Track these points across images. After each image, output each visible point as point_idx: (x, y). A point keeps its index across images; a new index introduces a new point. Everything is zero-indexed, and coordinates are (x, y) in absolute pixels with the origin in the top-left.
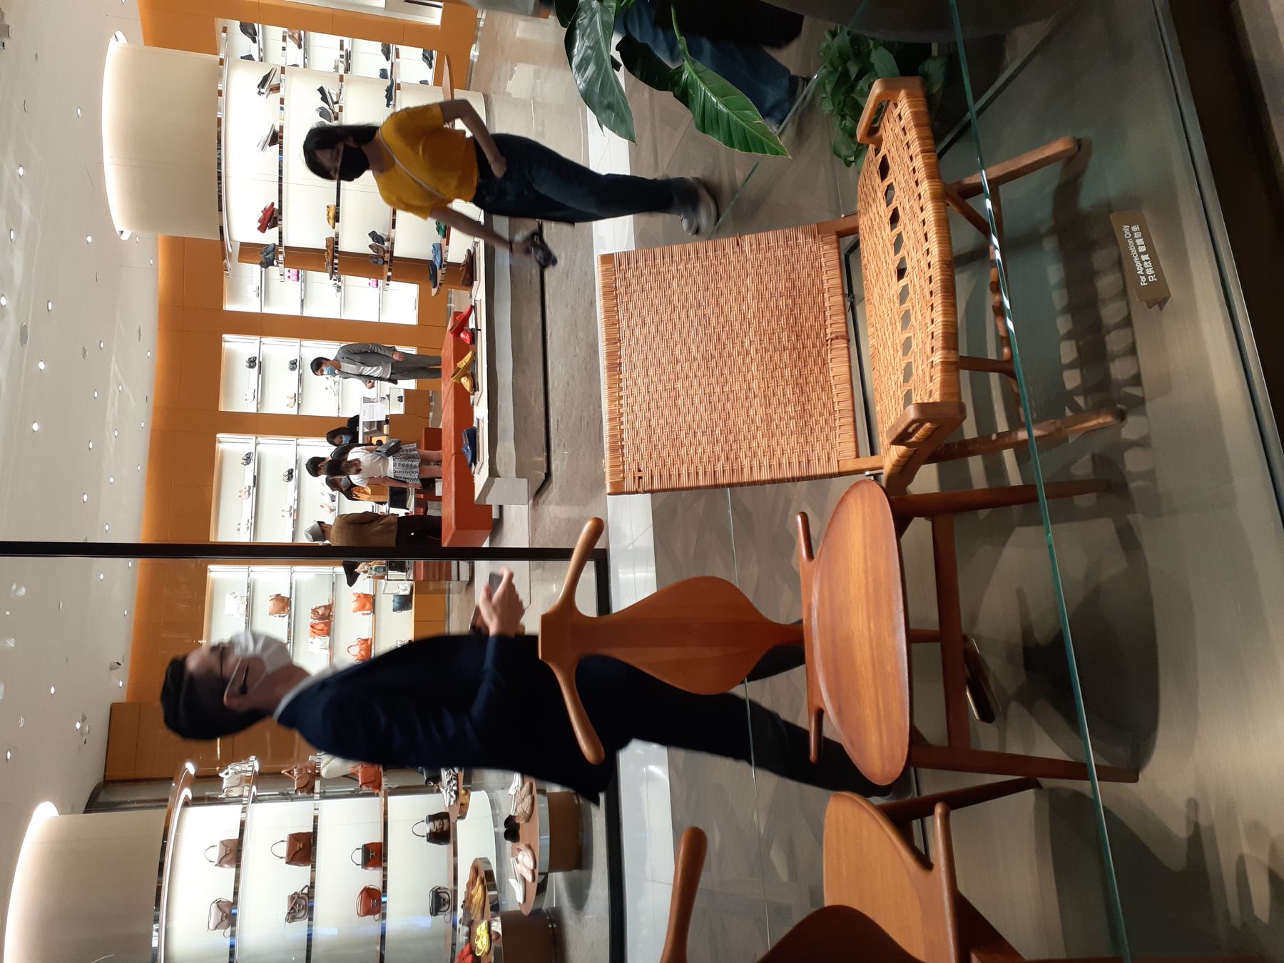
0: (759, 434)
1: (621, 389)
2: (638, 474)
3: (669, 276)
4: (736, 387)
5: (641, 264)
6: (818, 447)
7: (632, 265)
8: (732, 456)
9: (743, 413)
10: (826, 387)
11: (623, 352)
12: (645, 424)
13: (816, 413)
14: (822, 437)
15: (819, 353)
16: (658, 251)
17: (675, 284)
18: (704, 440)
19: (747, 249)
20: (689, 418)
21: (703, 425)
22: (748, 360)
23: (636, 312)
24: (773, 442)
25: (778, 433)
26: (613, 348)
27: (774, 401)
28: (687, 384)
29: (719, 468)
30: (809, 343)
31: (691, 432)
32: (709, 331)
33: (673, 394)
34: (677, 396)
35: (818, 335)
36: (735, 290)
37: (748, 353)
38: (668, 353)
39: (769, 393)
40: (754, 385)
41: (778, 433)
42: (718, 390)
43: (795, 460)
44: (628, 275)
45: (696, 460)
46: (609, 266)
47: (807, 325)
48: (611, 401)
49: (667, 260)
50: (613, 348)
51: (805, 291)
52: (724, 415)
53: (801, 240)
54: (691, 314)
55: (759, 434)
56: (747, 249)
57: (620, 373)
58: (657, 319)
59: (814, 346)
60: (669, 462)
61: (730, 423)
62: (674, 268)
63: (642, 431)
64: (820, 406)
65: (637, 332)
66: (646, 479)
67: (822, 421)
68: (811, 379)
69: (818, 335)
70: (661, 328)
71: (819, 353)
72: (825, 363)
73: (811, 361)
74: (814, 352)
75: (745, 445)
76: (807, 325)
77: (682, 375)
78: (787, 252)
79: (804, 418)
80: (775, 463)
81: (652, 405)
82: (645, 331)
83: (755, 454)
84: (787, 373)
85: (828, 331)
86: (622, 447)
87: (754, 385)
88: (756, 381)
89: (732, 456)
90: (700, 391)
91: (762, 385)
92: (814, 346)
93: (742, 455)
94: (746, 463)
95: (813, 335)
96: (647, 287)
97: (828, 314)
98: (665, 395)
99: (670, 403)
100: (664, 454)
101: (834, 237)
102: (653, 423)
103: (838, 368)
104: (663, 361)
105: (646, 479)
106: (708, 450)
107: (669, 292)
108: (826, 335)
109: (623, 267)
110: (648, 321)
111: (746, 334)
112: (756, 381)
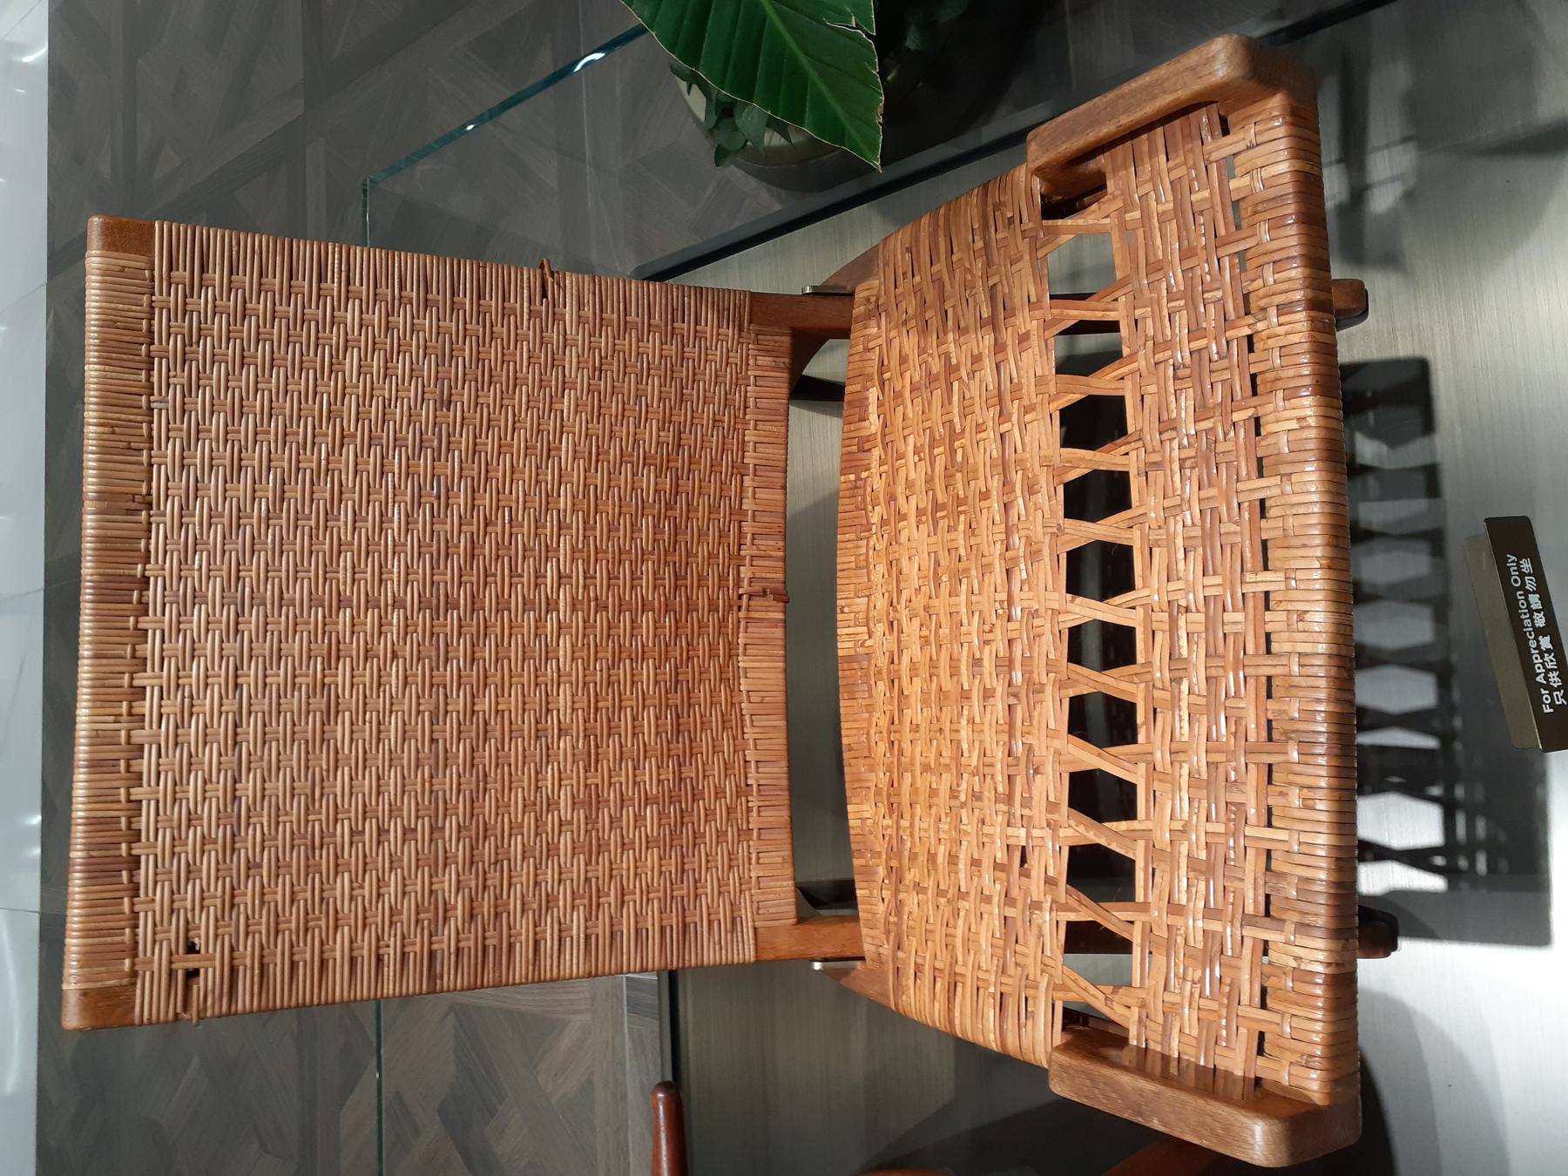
0: (565, 842)
1: (140, 663)
2: (186, 963)
3: (335, 336)
4: (513, 701)
5: (246, 279)
6: (710, 886)
7: (216, 275)
8: (486, 908)
9: (526, 777)
10: (732, 722)
11: (157, 540)
12: (219, 788)
13: (709, 793)
14: (721, 859)
15: (722, 623)
16: (307, 251)
17: (352, 361)
18: (408, 854)
19: (569, 313)
20: (367, 783)
21: (409, 807)
22: (550, 623)
23: (217, 423)
24: (601, 869)
25: (613, 840)
26: (123, 526)
27: (611, 748)
28: (367, 675)
29: (446, 940)
30: (703, 602)
31: (370, 828)
32: (448, 526)
33: (319, 702)
34: (331, 713)
35: (722, 579)
36: (528, 419)
37: (552, 606)
38: (313, 566)
39: (601, 725)
40: (563, 698)
41: (613, 840)
42: (459, 703)
43: (652, 924)
44: (200, 302)
45: (380, 914)
46: (134, 261)
47: (702, 552)
48: (101, 700)
49: (333, 286)
50: (123, 526)
51: (705, 462)
52: (469, 785)
53: (708, 329)
54: (396, 461)
55: (565, 842)
56: (569, 313)
57: (143, 609)
58: (283, 461)
59: (713, 608)
60: (293, 918)
61: (488, 805)
62: (351, 315)
63: (207, 811)
64: (716, 770)
65: (214, 484)
66: (211, 977)
67: (720, 810)
68: (702, 695)
69: (722, 579)
70: (295, 491)
71: (722, 623)
72: (731, 655)
73: (702, 646)
74: (712, 622)
75: (524, 872)
76: (702, 552)
77: (354, 646)
78: (672, 350)
79: (680, 798)
80: (601, 928)
81: (250, 729)
82: (243, 488)
83: (551, 900)
84: (647, 669)
85: (745, 572)
86: (134, 862)
87: (563, 698)
88: (565, 690)
89: (486, 908)
90: (407, 703)
91: (582, 702)
92: (713, 608)
93: (515, 905)
94: (524, 927)
95: (712, 580)
96: (262, 352)
97: (748, 528)
98: (294, 702)
99: (313, 723)
100: (280, 894)
101: (786, 340)
102: (248, 787)
103: (761, 672)
104: (296, 593)
105: (211, 977)
106: (418, 886)
107: (329, 387)
108: (738, 584)
109: (181, 274)
110: (254, 458)
111: (550, 552)
112: (565, 690)
